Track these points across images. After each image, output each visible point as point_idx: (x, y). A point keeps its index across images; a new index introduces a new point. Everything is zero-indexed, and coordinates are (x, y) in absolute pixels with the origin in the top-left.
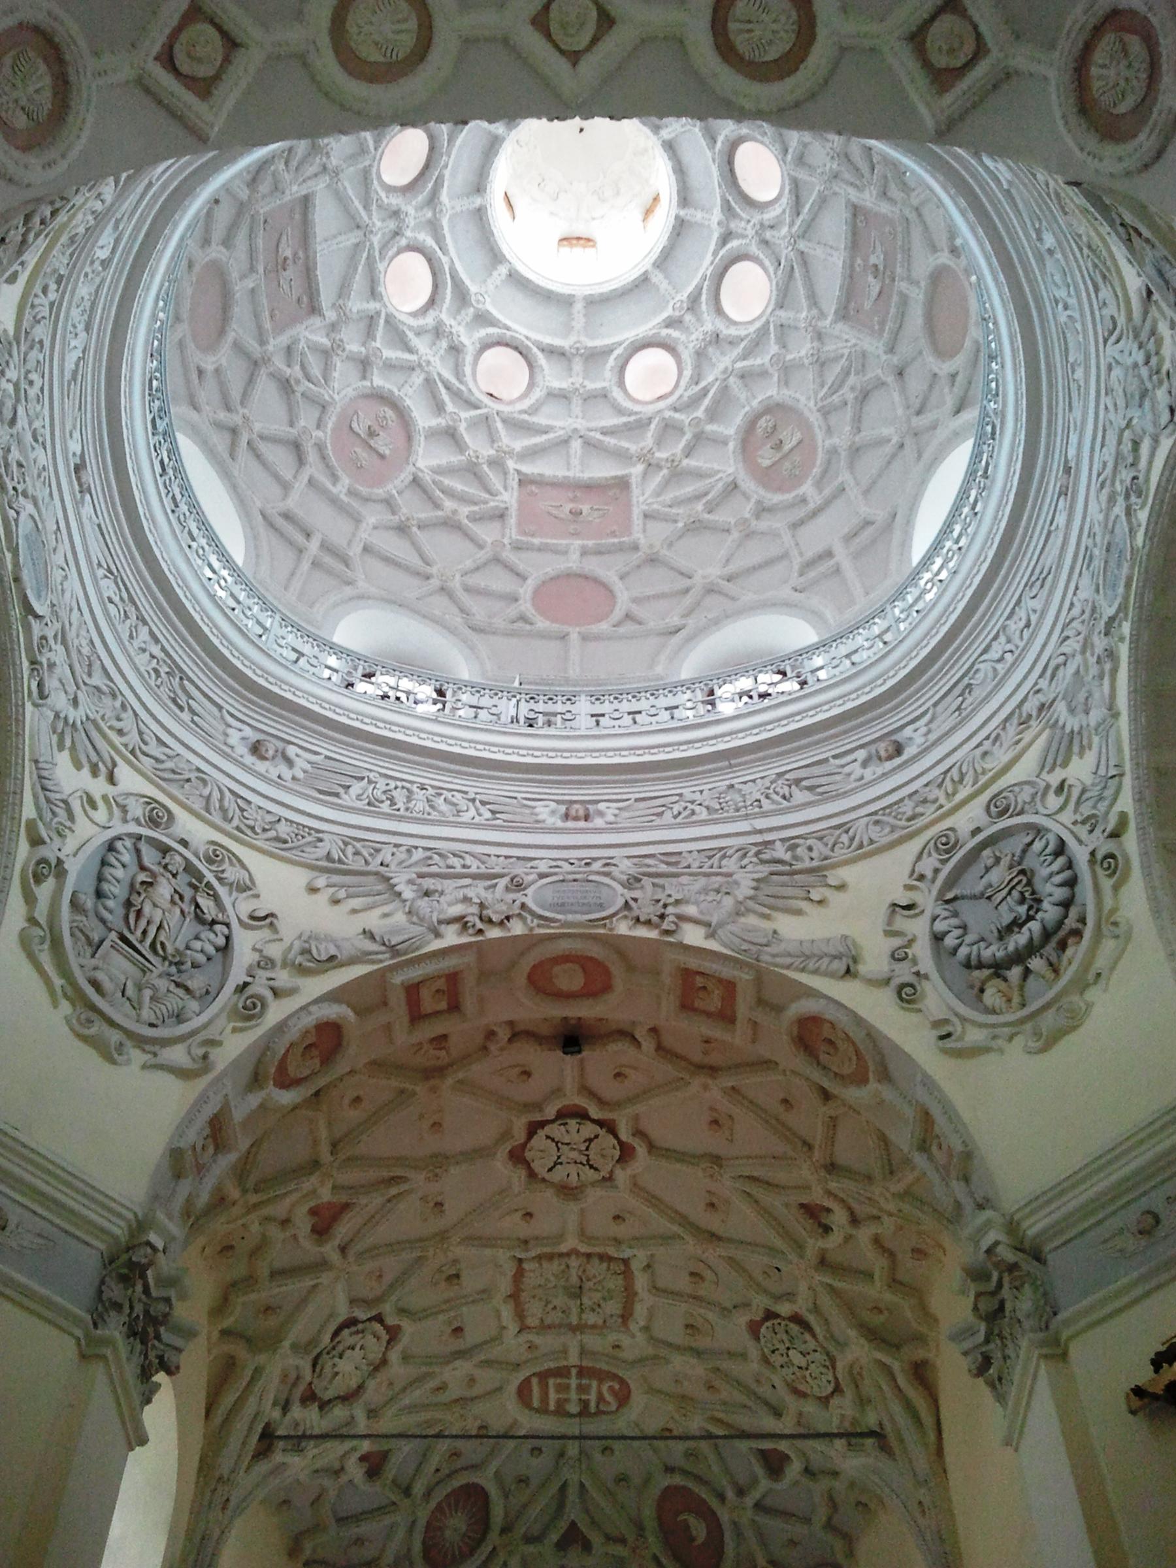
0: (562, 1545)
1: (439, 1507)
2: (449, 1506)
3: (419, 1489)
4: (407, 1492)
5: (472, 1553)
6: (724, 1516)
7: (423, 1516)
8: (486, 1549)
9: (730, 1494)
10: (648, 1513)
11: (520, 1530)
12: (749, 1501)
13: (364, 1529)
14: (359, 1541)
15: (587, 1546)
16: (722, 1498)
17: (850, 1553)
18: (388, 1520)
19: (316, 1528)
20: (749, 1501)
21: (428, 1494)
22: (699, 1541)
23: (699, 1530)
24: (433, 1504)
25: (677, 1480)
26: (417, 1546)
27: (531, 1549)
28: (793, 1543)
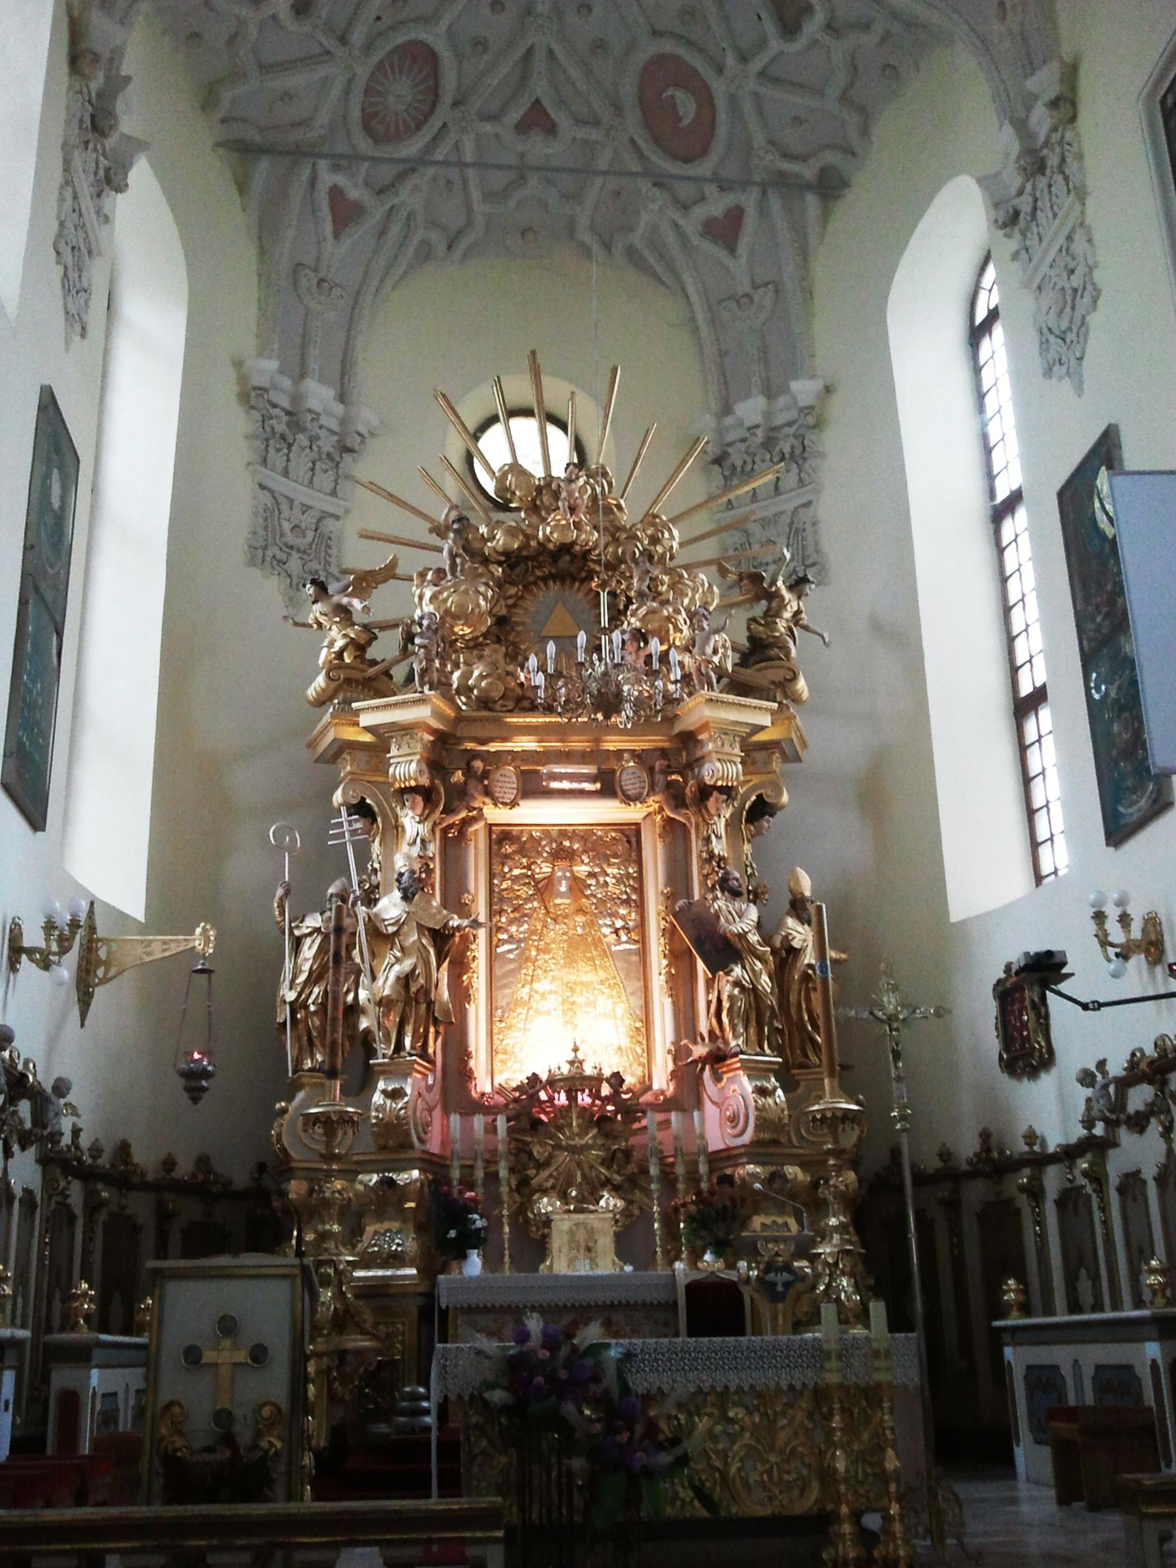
0: (522, 128)
1: (380, 66)
2: (392, 67)
3: (358, 36)
4: (343, 40)
5: (418, 128)
6: (719, 88)
7: (363, 71)
8: (435, 123)
9: (730, 61)
10: (628, 88)
11: (476, 104)
12: (756, 66)
13: (295, 81)
14: (287, 96)
15: (551, 129)
16: (720, 70)
17: (865, 131)
18: (321, 72)
19: (237, 75)
20: (756, 66)
21: (368, 48)
22: (687, 121)
23: (687, 107)
24: (376, 58)
25: (667, 46)
26: (356, 113)
27: (488, 128)
28: (798, 121)
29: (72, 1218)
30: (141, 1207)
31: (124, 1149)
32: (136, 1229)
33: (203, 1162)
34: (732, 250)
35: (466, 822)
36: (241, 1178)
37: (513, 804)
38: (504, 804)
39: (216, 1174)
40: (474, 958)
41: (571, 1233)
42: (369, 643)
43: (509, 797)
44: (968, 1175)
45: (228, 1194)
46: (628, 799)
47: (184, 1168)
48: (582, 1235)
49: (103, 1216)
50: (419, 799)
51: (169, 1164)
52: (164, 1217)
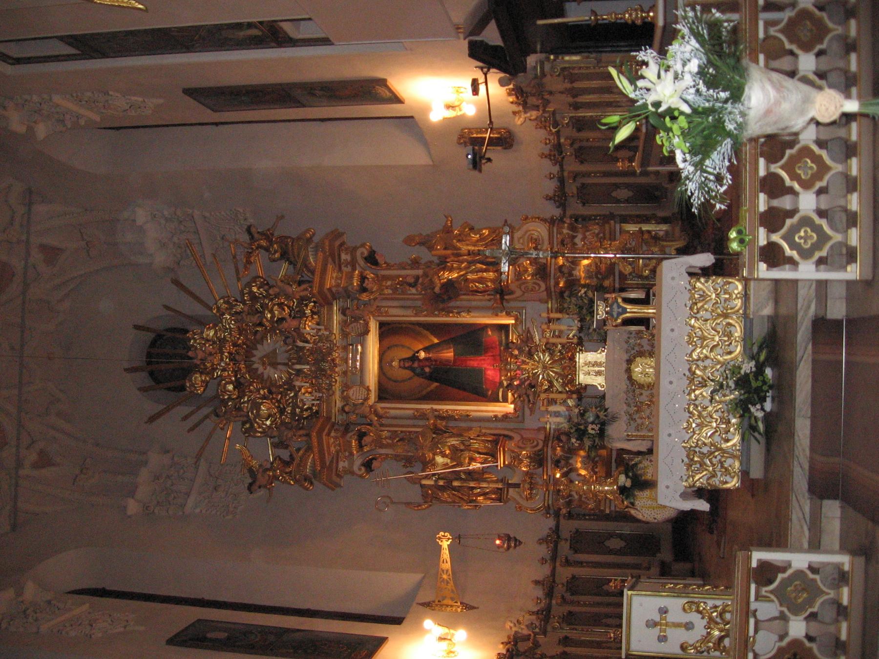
29: (570, 612)
30: (565, 573)
31: (537, 582)
32: (573, 577)
33: (541, 541)
34: (59, 250)
35: (376, 414)
36: (551, 522)
37: (368, 389)
38: (368, 394)
39: (548, 536)
40: (447, 411)
41: (585, 374)
42: (280, 459)
43: (365, 392)
44: (561, 166)
45: (557, 530)
46: (367, 332)
47: (544, 551)
48: (586, 368)
49: (568, 596)
50: (365, 438)
51: (543, 561)
52: (568, 563)
